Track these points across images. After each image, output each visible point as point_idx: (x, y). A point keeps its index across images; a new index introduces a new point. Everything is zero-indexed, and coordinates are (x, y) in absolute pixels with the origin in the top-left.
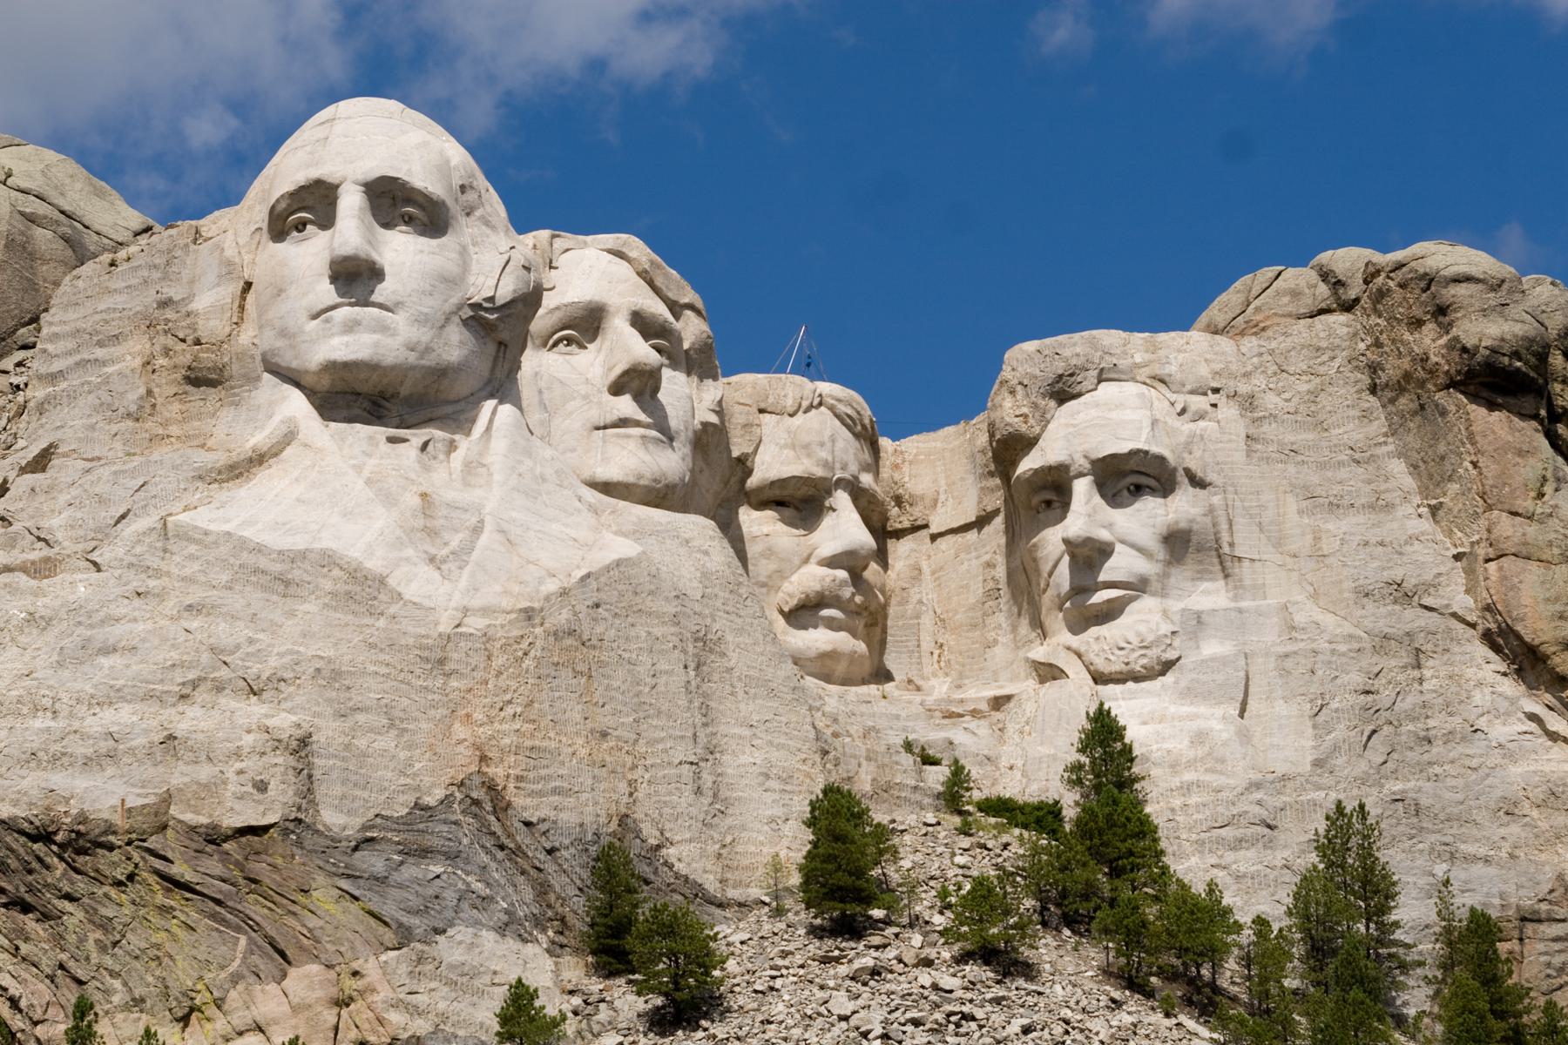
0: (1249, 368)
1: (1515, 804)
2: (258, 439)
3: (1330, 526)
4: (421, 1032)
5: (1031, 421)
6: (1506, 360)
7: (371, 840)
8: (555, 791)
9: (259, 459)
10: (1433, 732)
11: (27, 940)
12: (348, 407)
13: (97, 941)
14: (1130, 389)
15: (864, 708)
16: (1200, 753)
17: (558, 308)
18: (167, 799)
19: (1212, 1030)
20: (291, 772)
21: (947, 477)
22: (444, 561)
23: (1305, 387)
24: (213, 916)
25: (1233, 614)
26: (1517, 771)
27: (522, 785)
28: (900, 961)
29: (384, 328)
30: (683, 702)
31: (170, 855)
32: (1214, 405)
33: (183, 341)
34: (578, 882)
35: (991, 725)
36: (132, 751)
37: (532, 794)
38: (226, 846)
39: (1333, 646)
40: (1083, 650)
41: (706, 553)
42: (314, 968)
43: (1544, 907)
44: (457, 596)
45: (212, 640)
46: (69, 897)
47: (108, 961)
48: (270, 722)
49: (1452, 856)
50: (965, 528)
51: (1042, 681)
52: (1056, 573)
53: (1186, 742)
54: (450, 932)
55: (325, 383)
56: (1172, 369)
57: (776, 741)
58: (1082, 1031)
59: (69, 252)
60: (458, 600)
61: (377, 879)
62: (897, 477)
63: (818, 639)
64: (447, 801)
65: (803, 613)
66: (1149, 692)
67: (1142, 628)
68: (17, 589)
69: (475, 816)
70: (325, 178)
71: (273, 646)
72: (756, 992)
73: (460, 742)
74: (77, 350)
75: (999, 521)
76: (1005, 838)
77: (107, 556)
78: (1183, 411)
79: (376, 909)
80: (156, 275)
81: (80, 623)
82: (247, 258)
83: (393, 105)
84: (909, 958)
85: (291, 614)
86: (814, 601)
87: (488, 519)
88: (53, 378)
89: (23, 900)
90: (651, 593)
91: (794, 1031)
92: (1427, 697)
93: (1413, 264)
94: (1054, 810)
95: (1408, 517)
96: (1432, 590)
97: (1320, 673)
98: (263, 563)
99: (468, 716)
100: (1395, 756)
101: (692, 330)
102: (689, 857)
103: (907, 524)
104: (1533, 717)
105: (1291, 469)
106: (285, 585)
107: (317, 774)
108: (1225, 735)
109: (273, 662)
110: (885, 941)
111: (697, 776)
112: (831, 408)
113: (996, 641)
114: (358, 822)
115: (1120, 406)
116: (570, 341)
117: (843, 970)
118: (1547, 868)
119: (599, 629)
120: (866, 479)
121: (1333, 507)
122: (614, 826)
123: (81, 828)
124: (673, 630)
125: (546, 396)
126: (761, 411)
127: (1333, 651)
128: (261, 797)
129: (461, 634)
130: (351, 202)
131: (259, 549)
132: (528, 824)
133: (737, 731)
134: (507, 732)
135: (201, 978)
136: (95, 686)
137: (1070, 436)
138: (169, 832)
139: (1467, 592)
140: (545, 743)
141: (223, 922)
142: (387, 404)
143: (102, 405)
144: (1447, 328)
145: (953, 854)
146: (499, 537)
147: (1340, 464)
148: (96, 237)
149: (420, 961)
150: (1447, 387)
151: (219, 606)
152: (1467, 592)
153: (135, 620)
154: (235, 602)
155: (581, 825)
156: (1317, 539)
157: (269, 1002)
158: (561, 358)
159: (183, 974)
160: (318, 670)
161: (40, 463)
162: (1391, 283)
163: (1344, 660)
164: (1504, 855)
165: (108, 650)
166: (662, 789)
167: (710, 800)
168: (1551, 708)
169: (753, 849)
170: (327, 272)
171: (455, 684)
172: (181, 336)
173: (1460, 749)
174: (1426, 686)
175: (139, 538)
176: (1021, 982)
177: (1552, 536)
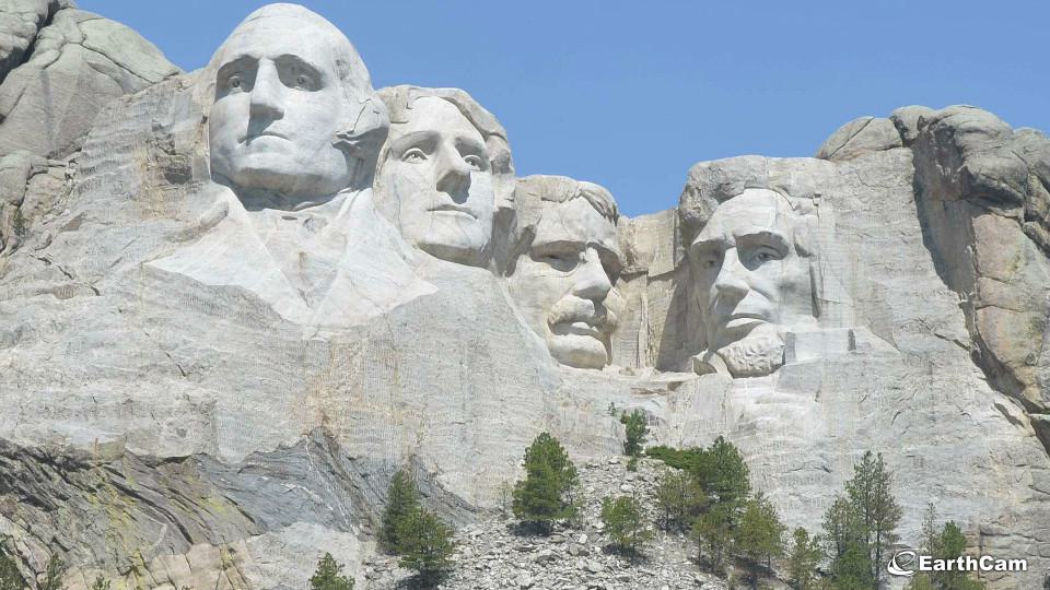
0: (843, 182)
2: (205, 215)
5: (702, 212)
6: (995, 183)
8: (372, 440)
9: (205, 227)
15: (592, 387)
16: (786, 424)
17: (409, 135)
22: (310, 295)
23: (876, 194)
24: (149, 512)
28: (569, 552)
29: (281, 149)
32: (817, 205)
33: (166, 152)
37: (356, 440)
38: (158, 468)
40: (726, 354)
41: (483, 292)
42: (206, 546)
43: (995, 526)
46: (64, 499)
53: (779, 416)
54: (294, 525)
55: (245, 181)
56: (792, 182)
60: (315, 321)
62: (629, 241)
63: (571, 341)
65: (562, 325)
66: (764, 383)
67: (762, 343)
72: (477, 569)
73: (311, 408)
77: (105, 285)
78: (798, 207)
79: (246, 510)
80: (154, 109)
81: (82, 328)
87: (340, 270)
89: (34, 497)
98: (199, 293)
101: (495, 149)
102: (454, 481)
103: (634, 271)
104: (1000, 407)
106: (212, 309)
107: (219, 426)
108: (803, 413)
109: (197, 355)
110: (562, 539)
112: (587, 198)
114: (243, 456)
116: (416, 155)
117: (533, 556)
118: (1000, 503)
120: (609, 243)
121: (888, 271)
122: (405, 462)
123: (70, 455)
124: (455, 340)
125: (399, 189)
126: (543, 199)
127: (877, 363)
128: (181, 439)
131: (197, 285)
132: (351, 459)
133: (492, 402)
134: (341, 402)
135: (138, 550)
136: (87, 368)
137: (723, 222)
141: (154, 515)
147: (896, 244)
148: (138, 79)
149: (272, 543)
151: (169, 320)
153: (117, 327)
155: (384, 460)
157: (178, 565)
159: (128, 547)
160: (224, 362)
161: (74, 225)
162: (932, 132)
163: (883, 368)
169: (497, 476)
177: (1020, 294)
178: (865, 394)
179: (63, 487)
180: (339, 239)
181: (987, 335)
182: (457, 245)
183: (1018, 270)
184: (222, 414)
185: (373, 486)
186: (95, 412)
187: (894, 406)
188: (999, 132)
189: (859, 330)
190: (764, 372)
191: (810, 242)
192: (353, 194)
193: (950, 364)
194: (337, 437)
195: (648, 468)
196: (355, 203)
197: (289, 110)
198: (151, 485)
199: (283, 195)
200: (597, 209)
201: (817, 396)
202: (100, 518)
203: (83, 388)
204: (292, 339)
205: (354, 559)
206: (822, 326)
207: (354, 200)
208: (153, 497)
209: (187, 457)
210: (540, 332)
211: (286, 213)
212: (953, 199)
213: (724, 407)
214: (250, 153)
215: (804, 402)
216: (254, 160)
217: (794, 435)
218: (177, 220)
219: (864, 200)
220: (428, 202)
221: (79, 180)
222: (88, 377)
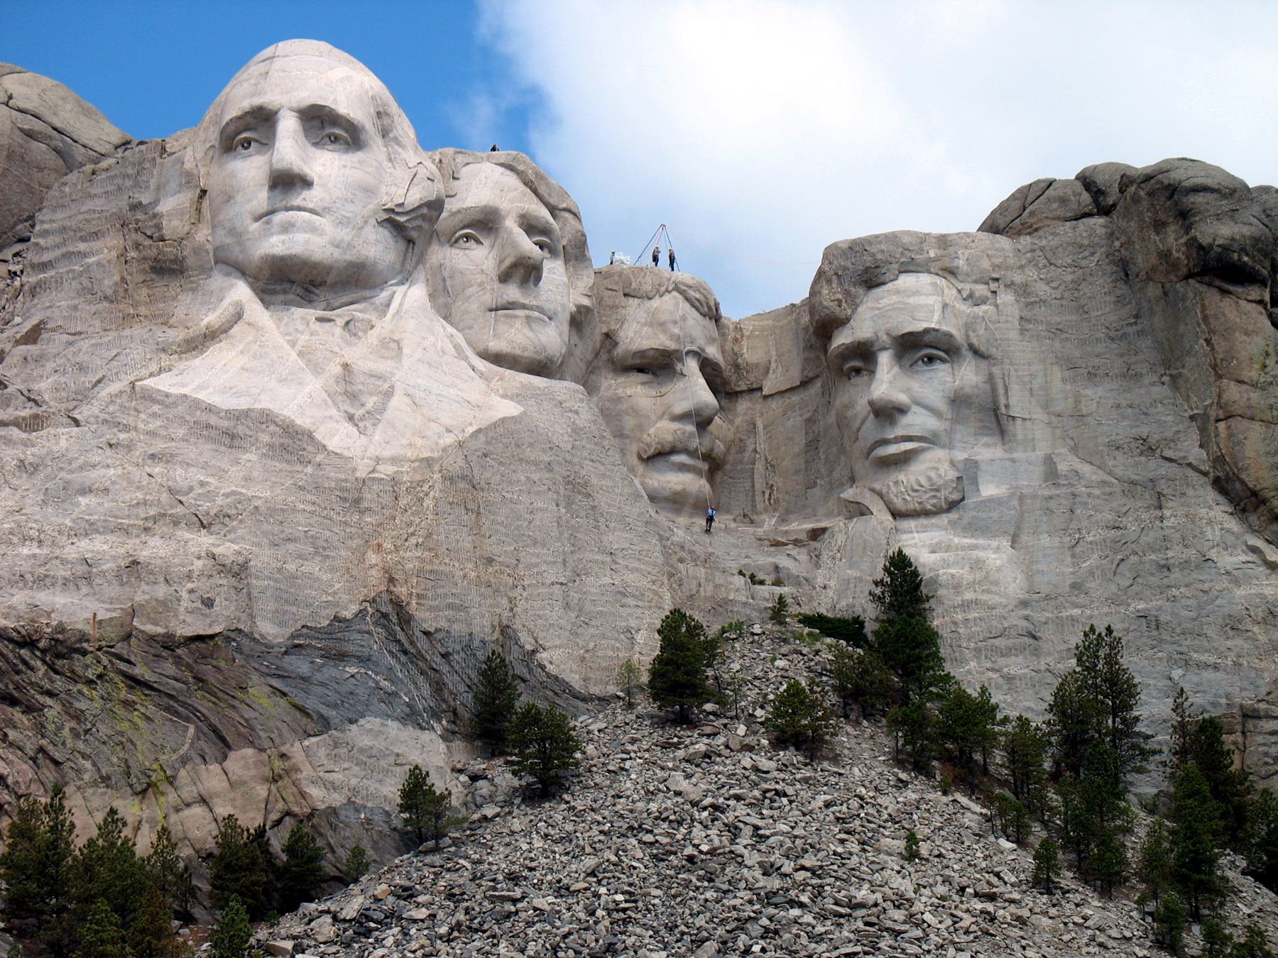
1: (1240, 621)
2: (211, 318)
3: (1089, 392)
4: (336, 804)
5: (844, 304)
6: (1236, 256)
7: (297, 646)
8: (450, 606)
9: (212, 336)
10: (1172, 561)
11: (15, 727)
12: (285, 292)
13: (72, 729)
14: (925, 279)
17: (459, 211)
18: (133, 613)
19: (984, 806)
20: (233, 591)
21: (777, 349)
23: (1069, 278)
24: (168, 709)
25: (1008, 463)
26: (1240, 592)
27: (423, 601)
28: (727, 747)
29: (313, 229)
30: (555, 533)
31: (133, 659)
33: (151, 237)
36: (103, 574)
37: (432, 609)
38: (179, 651)
39: (1089, 490)
40: (884, 491)
41: (576, 412)
42: (249, 751)
43: (1263, 706)
45: (170, 483)
46: (50, 694)
47: (81, 745)
48: (217, 551)
49: (1187, 663)
50: (792, 389)
51: (850, 518)
53: (967, 568)
54: (362, 722)
56: (961, 262)
57: (631, 566)
58: (874, 805)
59: (60, 162)
60: (373, 451)
61: (303, 678)
62: (736, 349)
64: (361, 614)
67: (933, 474)
68: (10, 440)
69: (384, 626)
70: (265, 105)
72: (609, 771)
73: (371, 567)
74: (64, 244)
75: (818, 384)
76: (818, 645)
77: (86, 413)
78: (971, 296)
79: (297, 701)
80: (129, 183)
82: (203, 171)
83: (324, 46)
84: (735, 744)
86: (667, 449)
87: (398, 386)
88: (44, 266)
89: (11, 695)
90: (531, 445)
91: (638, 804)
92: (1167, 532)
93: (1160, 177)
94: (858, 622)
95: (1153, 384)
96: (1172, 445)
97: (1078, 511)
98: (213, 420)
99: (379, 545)
100: (1140, 580)
102: (559, 659)
103: (743, 386)
104: (1254, 550)
105: (1057, 345)
107: (255, 593)
110: (715, 730)
111: (566, 595)
112: (682, 293)
115: (916, 293)
116: (468, 237)
117: (681, 753)
118: (1266, 674)
119: (487, 475)
120: (712, 352)
122: (497, 635)
123: (60, 636)
124: (548, 475)
125: (448, 283)
126: (625, 295)
127: (1089, 495)
129: (374, 479)
130: (288, 126)
131: (210, 409)
132: (426, 633)
133: (599, 557)
134: (411, 558)
135: (157, 760)
136: (73, 521)
138: (133, 640)
139: (1201, 446)
141: (176, 713)
142: (317, 291)
143: (84, 289)
144: (1188, 229)
145: (774, 660)
146: (407, 400)
148: (83, 150)
149: (336, 745)
150: (1187, 277)
151: (177, 455)
152: (1201, 446)
154: (190, 452)
155: (471, 635)
156: (1077, 402)
158: (461, 253)
159: (142, 757)
161: (33, 336)
162: (1142, 193)
163: (1098, 502)
164: (1229, 663)
166: (537, 604)
168: (1270, 542)
171: (369, 519)
172: (149, 233)
173: (1195, 575)
175: (112, 399)
176: (826, 764)
179: (52, 681)
180: (393, 347)
181: (1233, 456)
183: (1268, 369)
184: (257, 578)
186: (88, 578)
187: (1116, 552)
188: (1235, 191)
189: (1060, 454)
190: (937, 512)
191: (988, 341)
192: (402, 289)
193: (1184, 494)
194: (408, 604)
196: (407, 299)
197: (320, 177)
200: (697, 309)
201: (1014, 542)
202: (103, 721)
203: (68, 549)
205: (442, 764)
206: (1010, 450)
207: (405, 295)
208: (174, 689)
209: (216, 635)
211: (320, 313)
212: (1175, 279)
214: (272, 234)
215: (998, 548)
216: (276, 245)
217: (989, 591)
219: (1054, 284)
220: (488, 299)
221: (31, 279)
222: (75, 534)
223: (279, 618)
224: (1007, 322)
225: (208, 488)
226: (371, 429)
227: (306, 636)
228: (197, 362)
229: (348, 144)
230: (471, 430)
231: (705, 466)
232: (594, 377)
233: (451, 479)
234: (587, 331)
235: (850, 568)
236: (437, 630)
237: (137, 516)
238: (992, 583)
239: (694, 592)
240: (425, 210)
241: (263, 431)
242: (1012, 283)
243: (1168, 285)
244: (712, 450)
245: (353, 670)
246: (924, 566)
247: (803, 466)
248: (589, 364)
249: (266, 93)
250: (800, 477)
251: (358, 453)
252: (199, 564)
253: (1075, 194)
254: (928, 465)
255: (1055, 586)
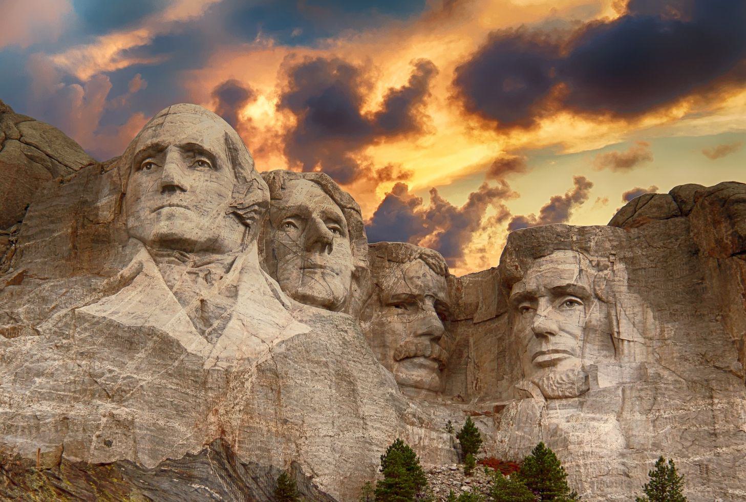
3: (670, 326)
7: (165, 470)
8: (260, 448)
12: (169, 256)
14: (570, 254)
17: (284, 209)
20: (124, 437)
23: (661, 255)
25: (617, 368)
29: (186, 219)
31: (61, 477)
34: (268, 494)
35: (494, 420)
40: (540, 383)
41: (346, 332)
44: (214, 351)
45: (91, 371)
48: (115, 412)
51: (519, 400)
52: (529, 345)
53: (587, 432)
57: (375, 426)
60: (215, 353)
61: (163, 491)
64: (204, 452)
67: (571, 375)
71: (121, 374)
77: (44, 327)
78: (598, 265)
85: (132, 358)
86: (412, 355)
90: (315, 351)
93: (717, 193)
97: (659, 399)
99: (217, 411)
102: (325, 482)
103: (463, 318)
107: (138, 438)
113: (503, 378)
120: (442, 295)
123: (18, 462)
125: (276, 252)
126: (389, 260)
128: (107, 449)
129: (215, 370)
131: (118, 326)
132: (244, 465)
134: (236, 419)
136: (31, 392)
138: (62, 466)
139: (739, 360)
140: (255, 425)
144: (733, 225)
150: (733, 255)
153: (55, 360)
155: (271, 466)
156: (662, 331)
162: (706, 203)
163: (671, 393)
165: (39, 374)
166: (314, 449)
167: (339, 454)
170: (161, 190)
171: (210, 395)
172: (91, 219)
174: (715, 407)
178: (657, 414)
180: (233, 292)
182: (323, 296)
184: (140, 429)
185: (262, 486)
187: (683, 424)
191: (608, 293)
194: (233, 446)
195: (480, 474)
198: (84, 486)
199: (186, 254)
200: (433, 270)
204: (195, 368)
208: (85, 496)
209: (113, 463)
210: (389, 368)
212: (725, 257)
213: (540, 425)
216: (163, 227)
218: (101, 276)
219: (651, 258)
220: (299, 262)
223: (153, 454)
224: (619, 281)
225: (113, 374)
226: (215, 339)
227: (169, 465)
228: (113, 297)
229: (209, 166)
230: (276, 341)
231: (436, 365)
232: (368, 310)
233: (263, 371)
234: (363, 283)
235: (518, 430)
236: (250, 463)
237: (70, 391)
238: (602, 442)
239: (417, 443)
240: (256, 207)
241: (150, 340)
242: (625, 258)
243: (721, 260)
244: (440, 356)
245: (196, 486)
246: (562, 430)
247: (496, 368)
248: (365, 302)
249: (160, 136)
250: (494, 374)
251: (207, 354)
252: (104, 420)
253: (667, 203)
254: (568, 368)
255: (642, 444)
